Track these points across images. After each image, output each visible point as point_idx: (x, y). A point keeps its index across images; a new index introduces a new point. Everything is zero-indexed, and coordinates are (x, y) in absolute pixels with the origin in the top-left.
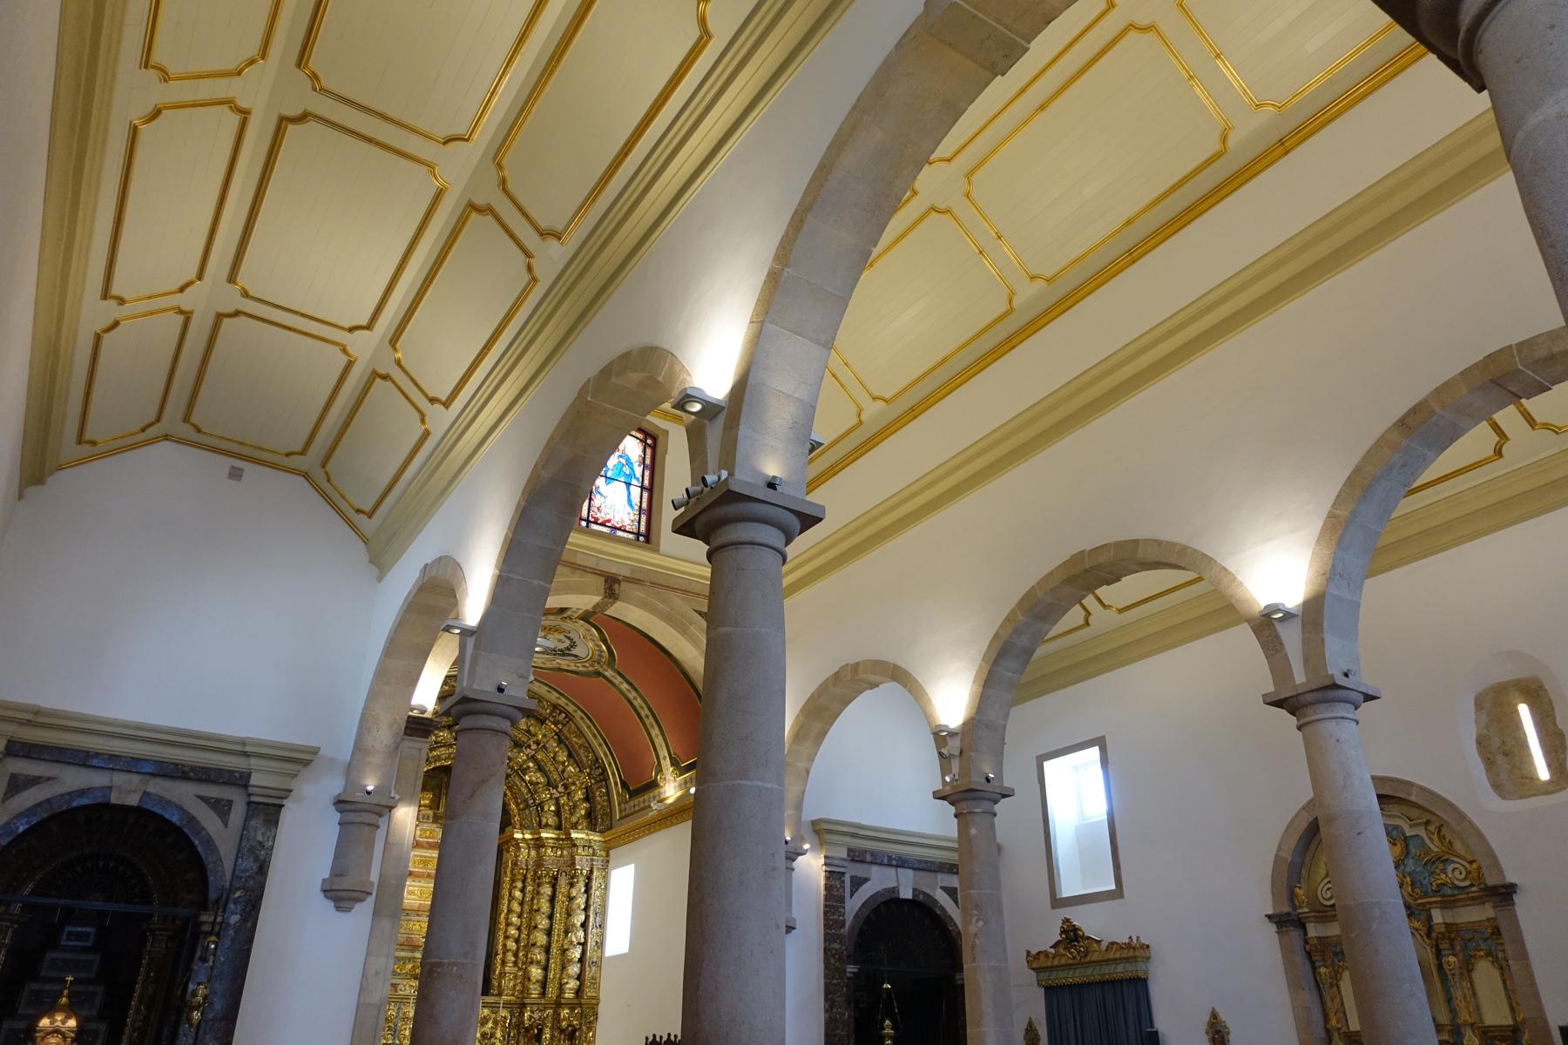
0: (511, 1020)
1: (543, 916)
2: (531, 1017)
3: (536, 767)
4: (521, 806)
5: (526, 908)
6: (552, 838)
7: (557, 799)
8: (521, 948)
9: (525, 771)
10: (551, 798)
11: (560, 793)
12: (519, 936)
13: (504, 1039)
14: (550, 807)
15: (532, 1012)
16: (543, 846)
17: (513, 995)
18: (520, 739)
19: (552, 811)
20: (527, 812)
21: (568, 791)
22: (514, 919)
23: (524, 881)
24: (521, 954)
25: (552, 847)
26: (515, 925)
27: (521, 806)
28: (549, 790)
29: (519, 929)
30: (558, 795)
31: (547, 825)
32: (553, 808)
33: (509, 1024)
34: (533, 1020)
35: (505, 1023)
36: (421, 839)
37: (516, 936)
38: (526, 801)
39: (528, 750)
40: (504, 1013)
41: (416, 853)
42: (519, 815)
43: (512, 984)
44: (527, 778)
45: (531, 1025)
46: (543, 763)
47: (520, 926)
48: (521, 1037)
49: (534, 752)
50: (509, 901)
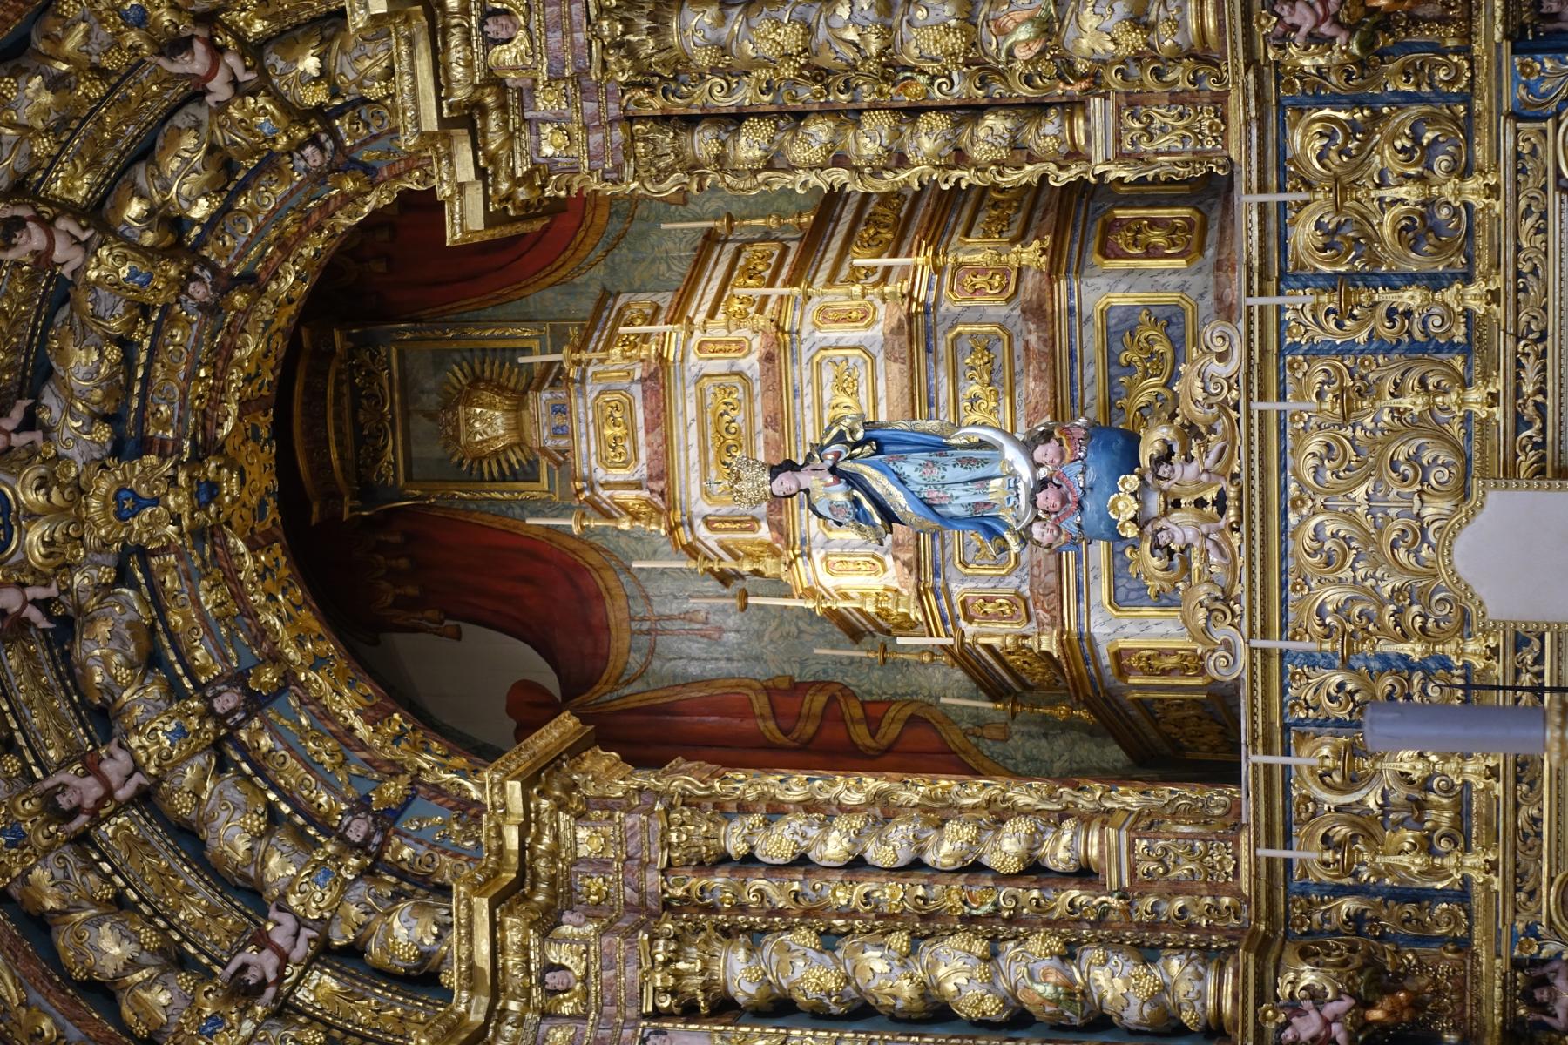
0: (1335, 102)
1: (822, 34)
2: (1314, 38)
3: (141, 175)
4: (349, 185)
5: (807, 94)
6: (440, 68)
7: (254, 50)
8: (998, 90)
9: (174, 223)
10: (264, 84)
11: (217, 52)
12: (941, 109)
13: (1430, 120)
14: (305, 80)
15: (1282, 42)
16: (494, 81)
17: (1219, 100)
18: (28, 300)
19: (322, 57)
20: (364, 155)
21: (185, 27)
22: (868, 142)
23: (690, 122)
24: (1025, 92)
25: (490, 42)
26: (897, 133)
27: (349, 185)
28: (223, 107)
29: (913, 112)
30: (231, 60)
31: (389, 73)
32: (310, 64)
33: (1356, 103)
34: (1325, 29)
35: (1351, 129)
36: (643, 455)
37: (939, 122)
38: (318, 178)
39: (58, 255)
40: (1305, 141)
41: (695, 490)
42: (398, 177)
43: (1162, 116)
44: (200, 210)
45: (1351, 29)
46: (109, 158)
47: (894, 110)
48: (1415, 37)
49: (63, 224)
50: (791, 169)
